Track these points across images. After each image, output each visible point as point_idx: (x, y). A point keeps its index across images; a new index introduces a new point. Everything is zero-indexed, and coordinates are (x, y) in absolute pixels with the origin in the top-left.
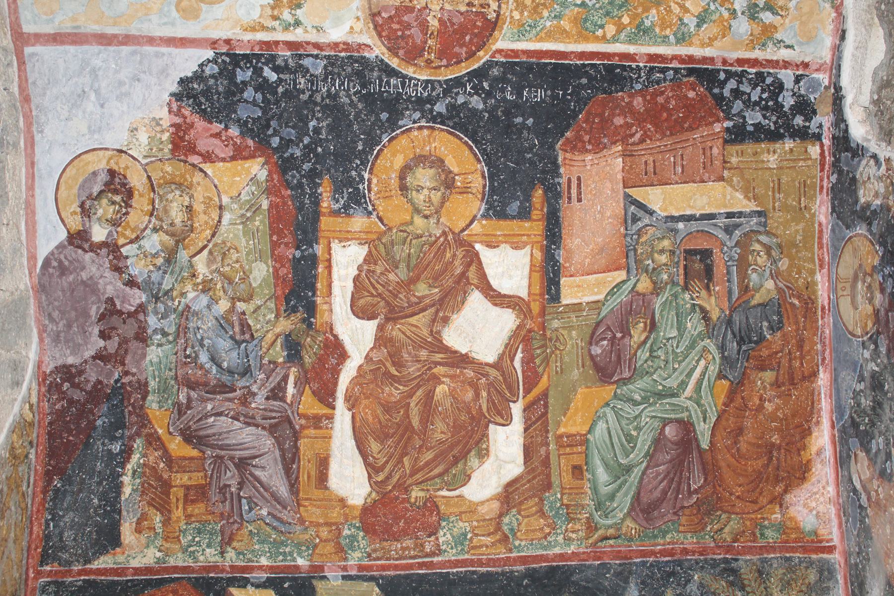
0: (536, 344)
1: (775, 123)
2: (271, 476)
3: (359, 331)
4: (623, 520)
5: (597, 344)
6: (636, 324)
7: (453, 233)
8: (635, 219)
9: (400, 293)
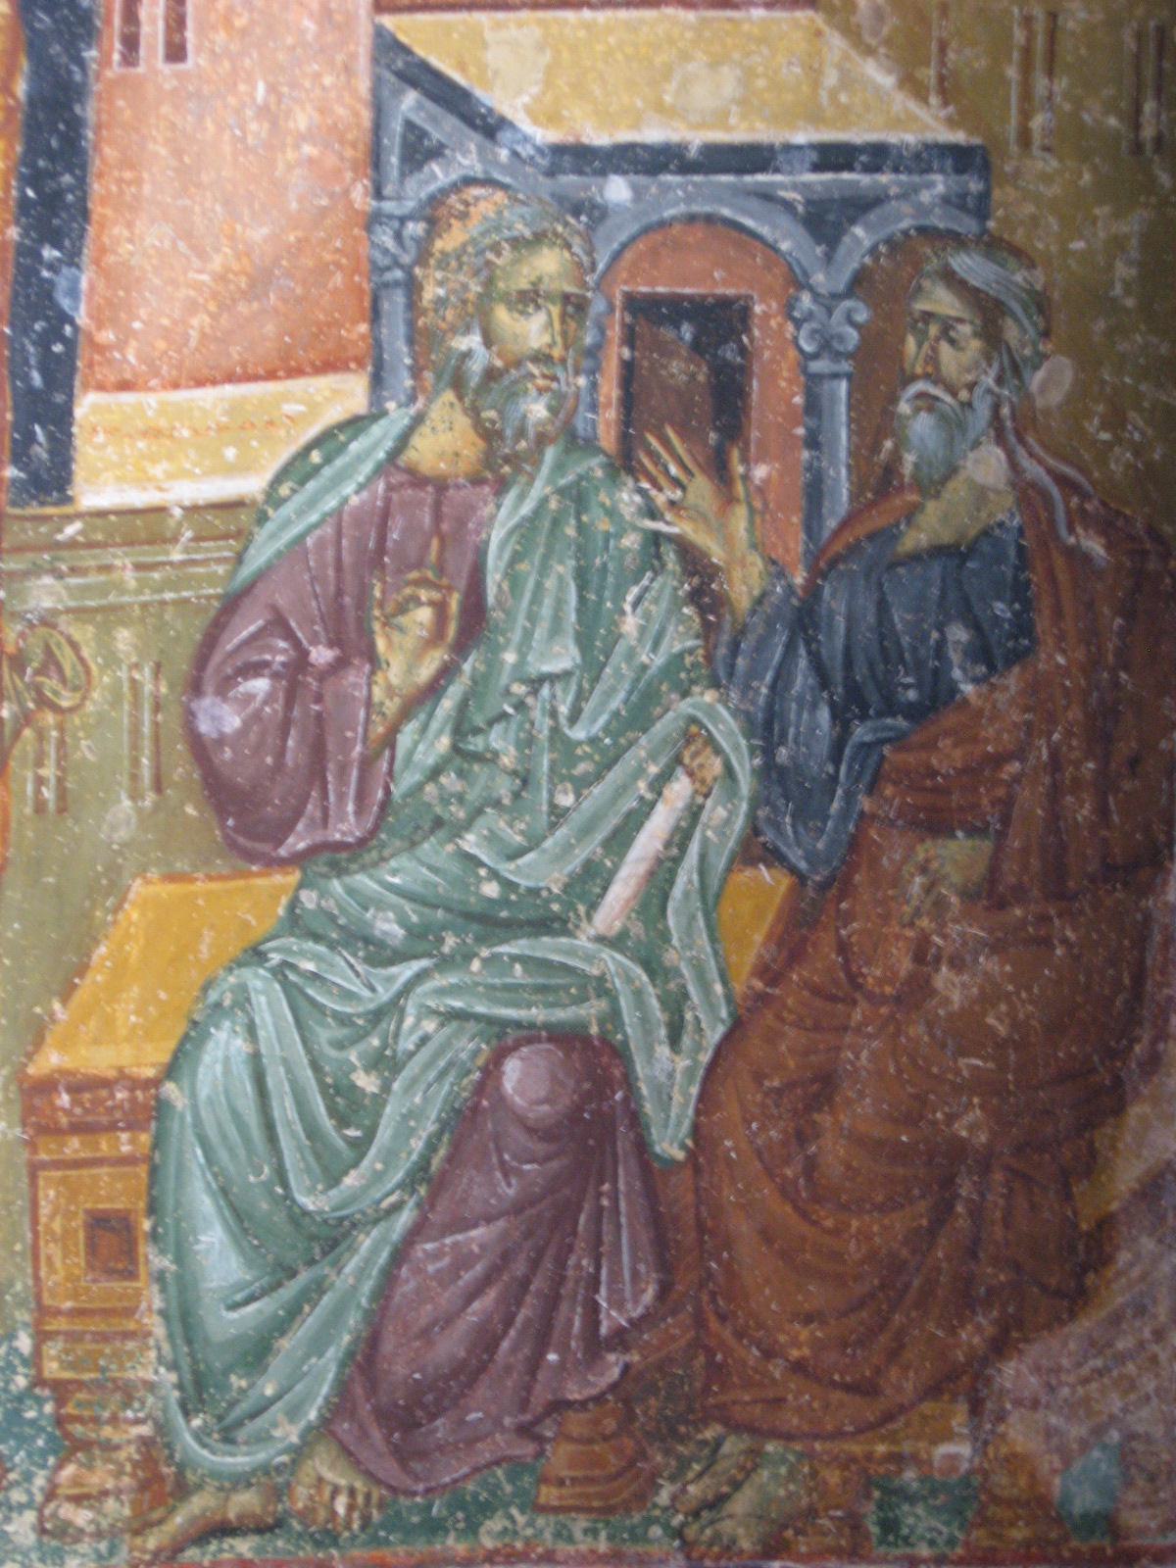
4: (300, 1453)
5: (224, 687)
6: (402, 609)
8: (419, 151)
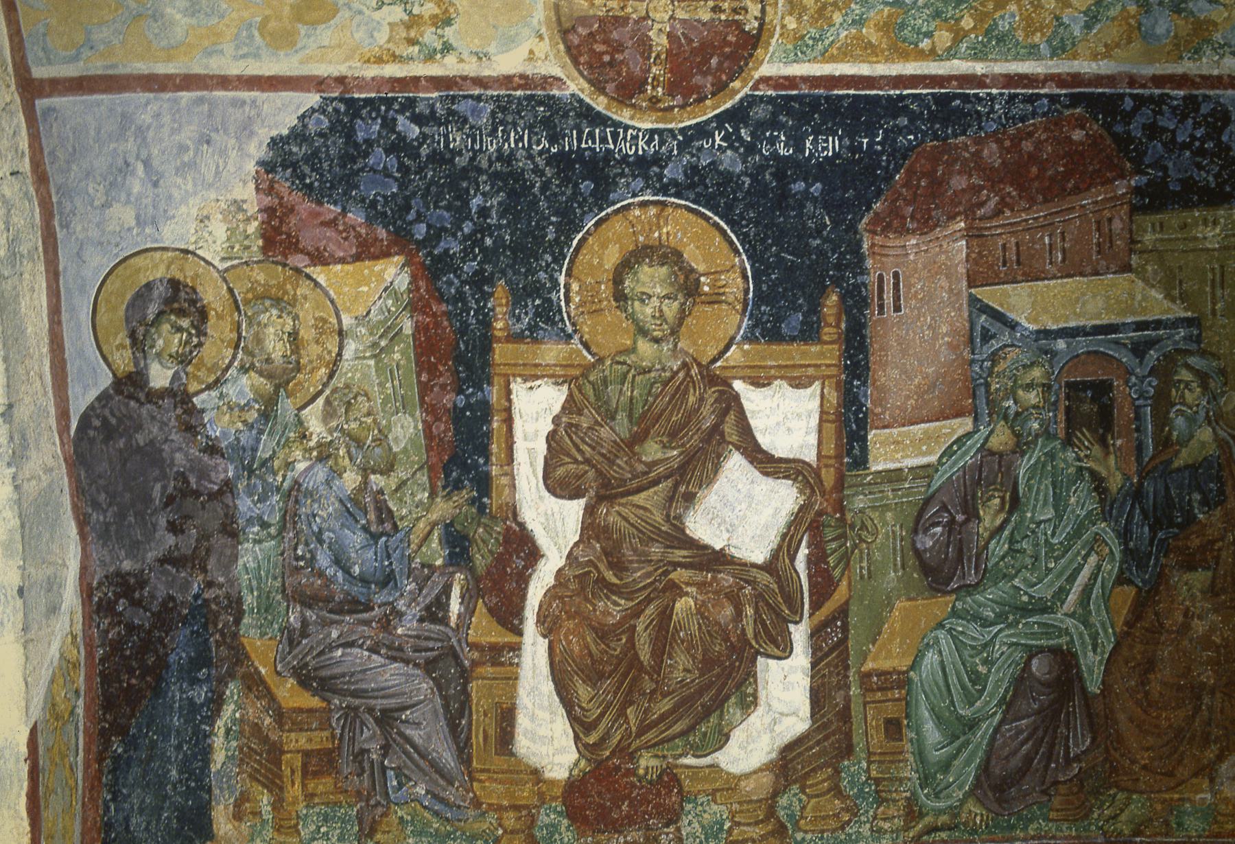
0: (829, 534)
1: (1216, 176)
2: (429, 737)
3: (557, 516)
4: (963, 802)
5: (926, 530)
6: (989, 500)
7: (699, 365)
8: (987, 337)
9: (617, 457)
